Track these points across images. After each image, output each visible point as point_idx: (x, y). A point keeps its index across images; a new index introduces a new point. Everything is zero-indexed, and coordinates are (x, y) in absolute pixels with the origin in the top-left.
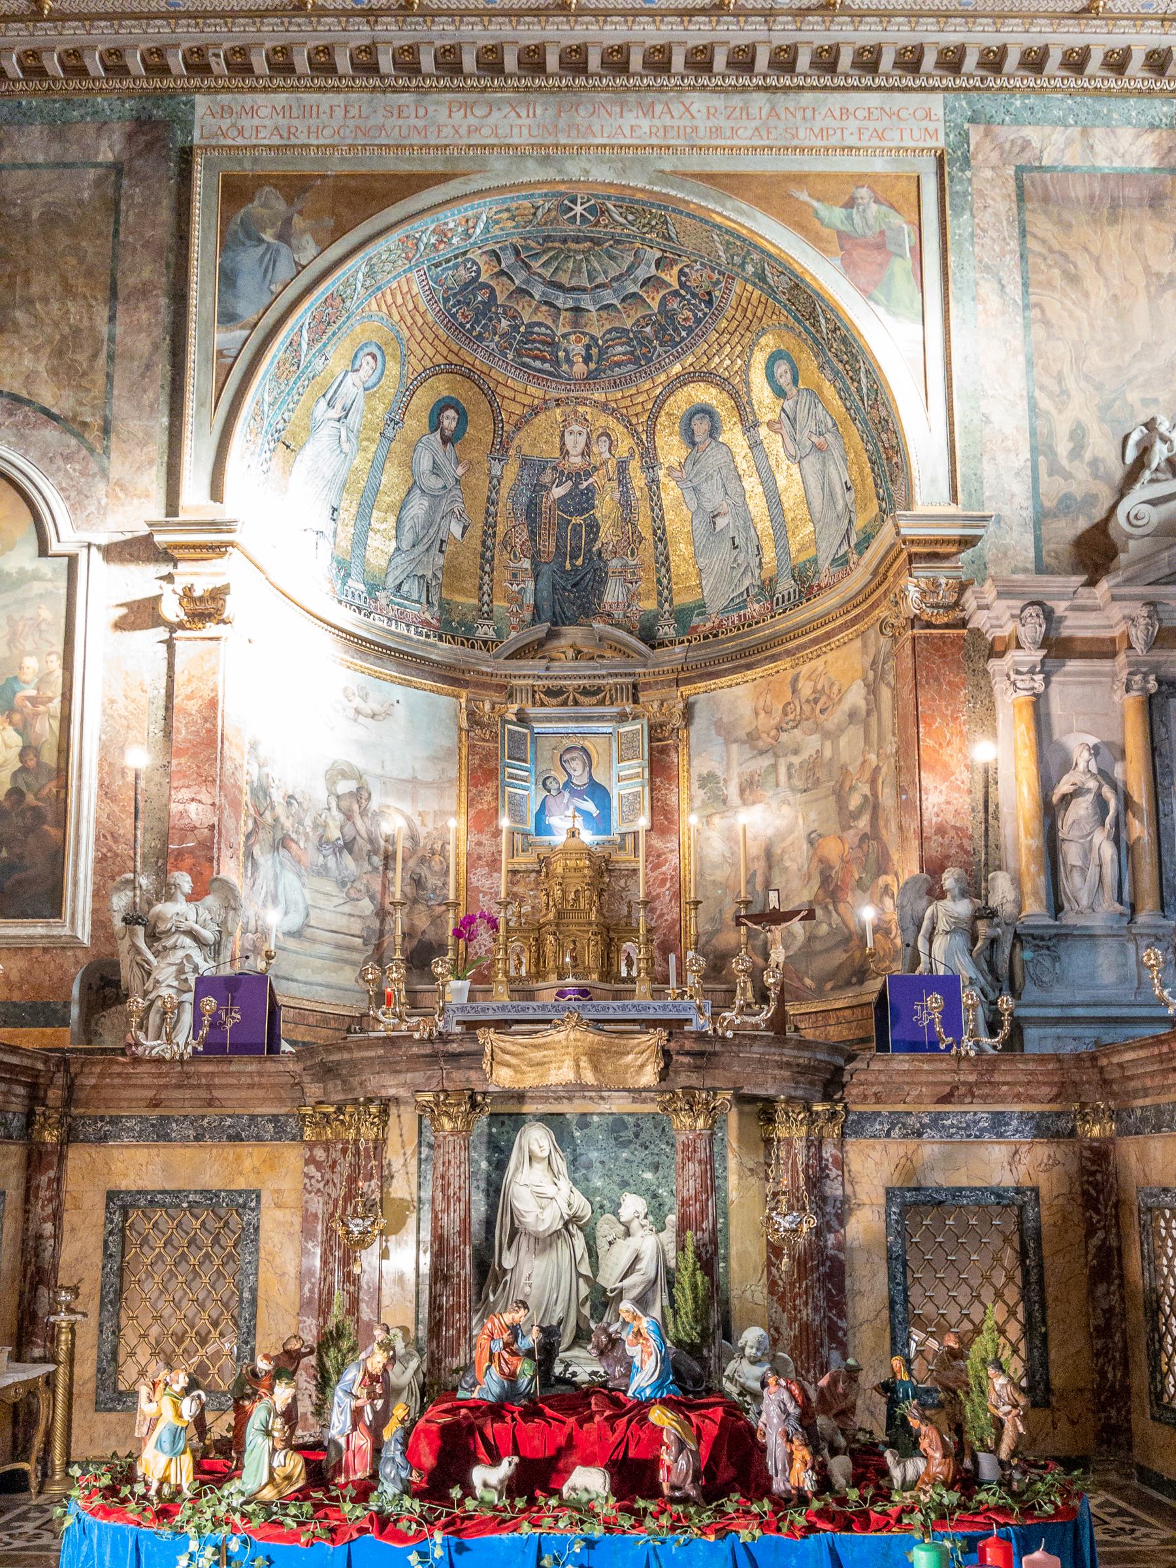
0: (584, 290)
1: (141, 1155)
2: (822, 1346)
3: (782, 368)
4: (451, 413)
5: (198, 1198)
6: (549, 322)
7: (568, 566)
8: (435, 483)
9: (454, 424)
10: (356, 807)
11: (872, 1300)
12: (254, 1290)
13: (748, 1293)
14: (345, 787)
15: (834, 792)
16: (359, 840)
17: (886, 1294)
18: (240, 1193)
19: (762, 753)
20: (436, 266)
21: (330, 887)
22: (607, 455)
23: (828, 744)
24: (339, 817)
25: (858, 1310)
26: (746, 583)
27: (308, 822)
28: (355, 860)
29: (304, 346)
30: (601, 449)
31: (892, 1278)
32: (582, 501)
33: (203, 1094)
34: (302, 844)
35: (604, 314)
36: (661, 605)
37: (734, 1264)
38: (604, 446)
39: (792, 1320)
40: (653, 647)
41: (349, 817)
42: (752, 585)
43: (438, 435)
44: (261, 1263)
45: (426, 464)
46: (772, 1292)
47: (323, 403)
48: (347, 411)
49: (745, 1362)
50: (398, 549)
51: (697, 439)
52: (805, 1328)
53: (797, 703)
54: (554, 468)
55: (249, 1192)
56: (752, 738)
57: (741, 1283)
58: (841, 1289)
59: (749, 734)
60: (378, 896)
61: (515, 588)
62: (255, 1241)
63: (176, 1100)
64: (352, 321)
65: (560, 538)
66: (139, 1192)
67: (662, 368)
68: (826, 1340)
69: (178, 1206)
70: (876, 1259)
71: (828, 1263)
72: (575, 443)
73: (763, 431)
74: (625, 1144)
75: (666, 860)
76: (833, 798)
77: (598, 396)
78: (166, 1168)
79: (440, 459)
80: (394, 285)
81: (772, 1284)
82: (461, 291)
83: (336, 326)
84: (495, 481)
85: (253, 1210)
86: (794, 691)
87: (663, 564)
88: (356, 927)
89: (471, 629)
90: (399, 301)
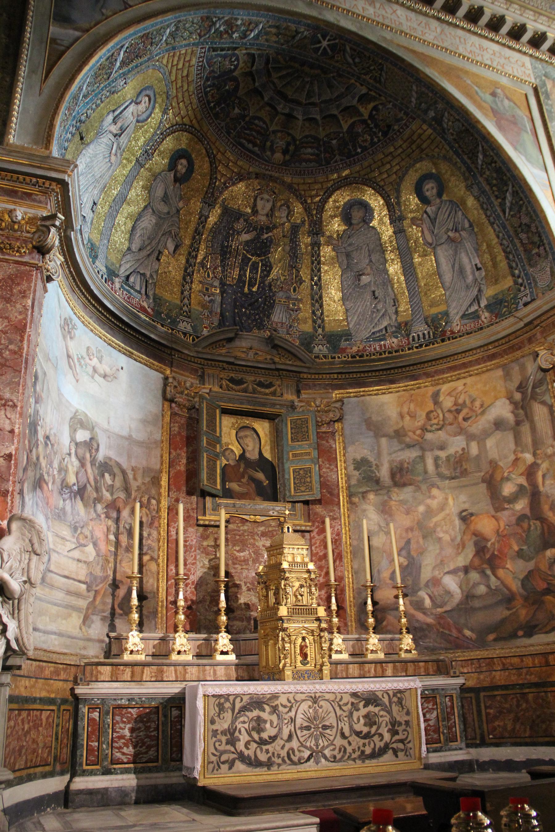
0: (299, 103)
16: (89, 488)
20: (214, 50)
24: (76, 463)
29: (118, 64)
35: (307, 125)
41: (83, 465)
64: (150, 63)
67: (337, 171)
73: (406, 223)
80: (183, 52)
82: (219, 76)
83: (140, 60)
90: (180, 66)
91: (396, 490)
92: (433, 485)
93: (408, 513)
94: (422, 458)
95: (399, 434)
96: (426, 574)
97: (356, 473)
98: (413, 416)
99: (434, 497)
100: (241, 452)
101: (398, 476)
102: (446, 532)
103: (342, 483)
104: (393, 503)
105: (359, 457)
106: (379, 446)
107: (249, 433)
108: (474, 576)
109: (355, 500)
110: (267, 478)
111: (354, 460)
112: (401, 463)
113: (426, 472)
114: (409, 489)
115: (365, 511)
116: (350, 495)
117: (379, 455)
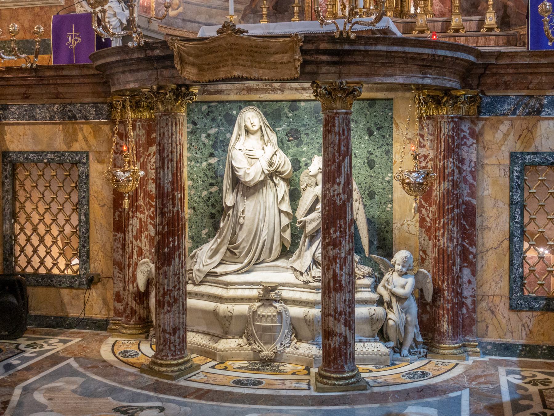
1: (20, 129)
2: (454, 264)
5: (53, 156)
11: (496, 233)
12: (87, 215)
13: (405, 226)
17: (507, 227)
18: (76, 153)
25: (486, 240)
31: (512, 218)
33: (54, 91)
37: (396, 206)
39: (435, 246)
44: (91, 198)
46: (421, 226)
49: (395, 274)
52: (442, 252)
55: (82, 153)
57: (400, 219)
58: (473, 225)
62: (87, 184)
63: (38, 94)
66: (20, 152)
68: (458, 261)
69: (41, 161)
70: (501, 204)
71: (464, 207)
78: (35, 137)
81: (422, 220)
85: (84, 164)
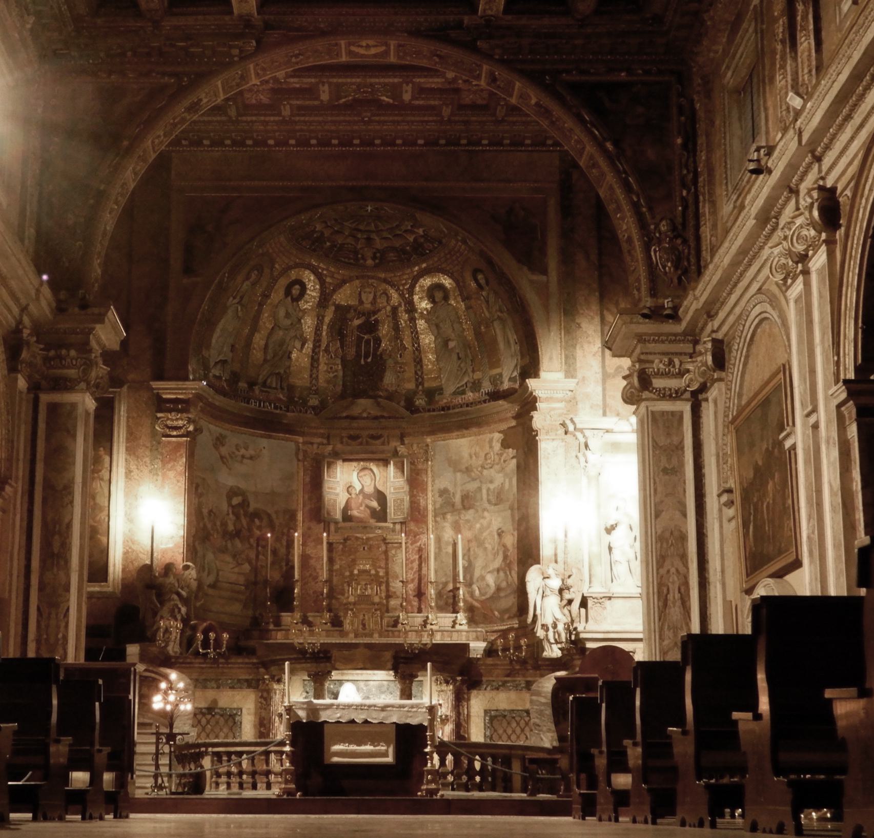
3: (480, 277)
4: (297, 287)
6: (353, 243)
7: (362, 362)
8: (288, 322)
9: (298, 292)
10: (242, 512)
14: (236, 501)
15: (510, 508)
19: (474, 480)
21: (228, 558)
22: (385, 304)
23: (507, 480)
26: (465, 380)
27: (218, 523)
28: (241, 542)
30: (382, 302)
32: (370, 327)
34: (215, 536)
36: (417, 386)
38: (384, 299)
40: (412, 412)
42: (468, 381)
43: (289, 298)
45: (282, 313)
47: (231, 299)
48: (242, 298)
50: (265, 360)
51: (437, 300)
53: (492, 453)
54: (355, 310)
56: (468, 470)
59: (467, 468)
60: (254, 562)
61: (331, 375)
65: (358, 346)
72: (367, 298)
74: (383, 693)
75: (419, 539)
76: (509, 511)
77: (383, 275)
79: (290, 311)
84: (320, 318)
86: (491, 447)
87: (418, 363)
88: (242, 580)
89: (305, 402)
91: (463, 512)
92: (484, 510)
93: (470, 529)
94: (480, 489)
95: (468, 470)
96: (477, 573)
97: (440, 499)
98: (477, 456)
99: (484, 518)
100: (361, 487)
101: (466, 501)
102: (490, 543)
103: (430, 507)
104: (461, 521)
105: (442, 487)
106: (456, 479)
107: (367, 472)
108: (502, 574)
109: (438, 519)
110: (379, 505)
111: (439, 489)
112: (468, 492)
113: (482, 499)
114: (471, 511)
115: (443, 527)
116: (435, 516)
117: (455, 485)
